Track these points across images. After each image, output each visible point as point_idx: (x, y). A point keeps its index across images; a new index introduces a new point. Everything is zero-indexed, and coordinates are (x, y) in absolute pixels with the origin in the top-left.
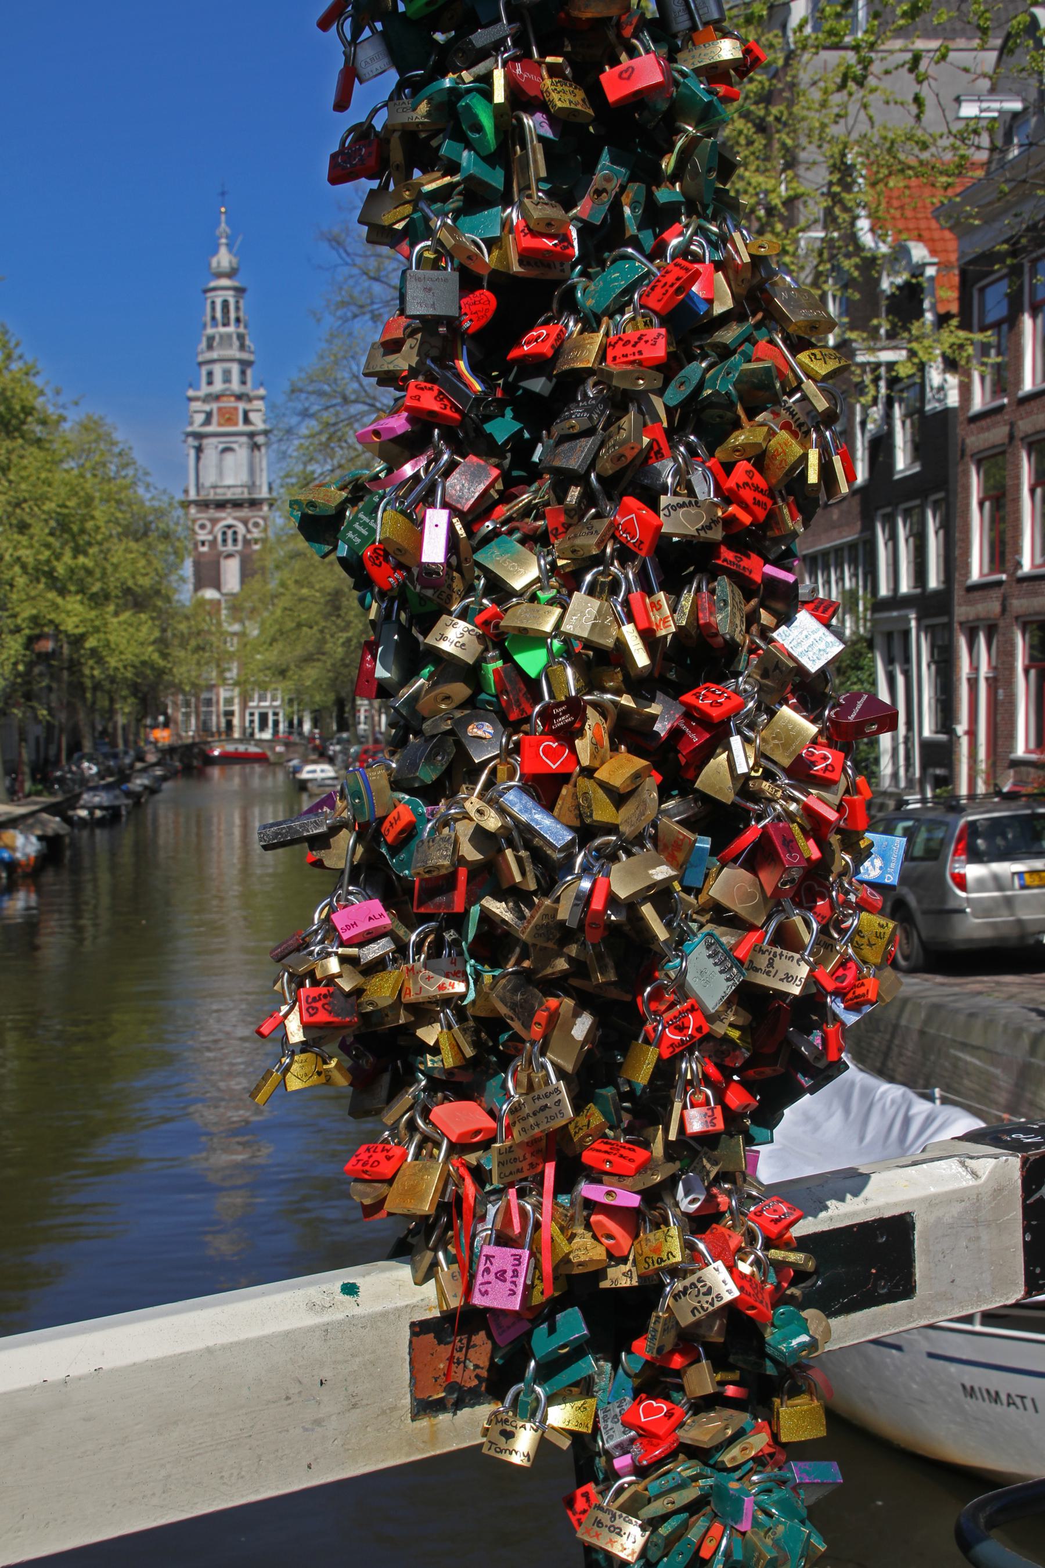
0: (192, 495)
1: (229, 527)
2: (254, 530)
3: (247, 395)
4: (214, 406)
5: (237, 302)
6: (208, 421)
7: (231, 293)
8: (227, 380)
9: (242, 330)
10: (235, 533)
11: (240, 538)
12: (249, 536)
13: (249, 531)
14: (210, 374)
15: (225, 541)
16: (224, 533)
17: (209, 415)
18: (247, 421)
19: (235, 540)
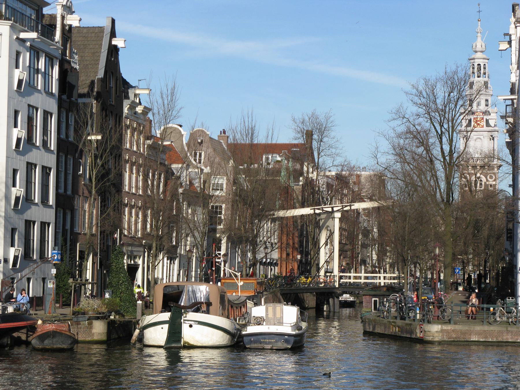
2: (490, 180)
3: (489, 112)
4: (472, 117)
7: (482, 60)
10: (481, 180)
11: (483, 183)
12: (487, 183)
13: (487, 180)
18: (488, 125)
19: (481, 184)
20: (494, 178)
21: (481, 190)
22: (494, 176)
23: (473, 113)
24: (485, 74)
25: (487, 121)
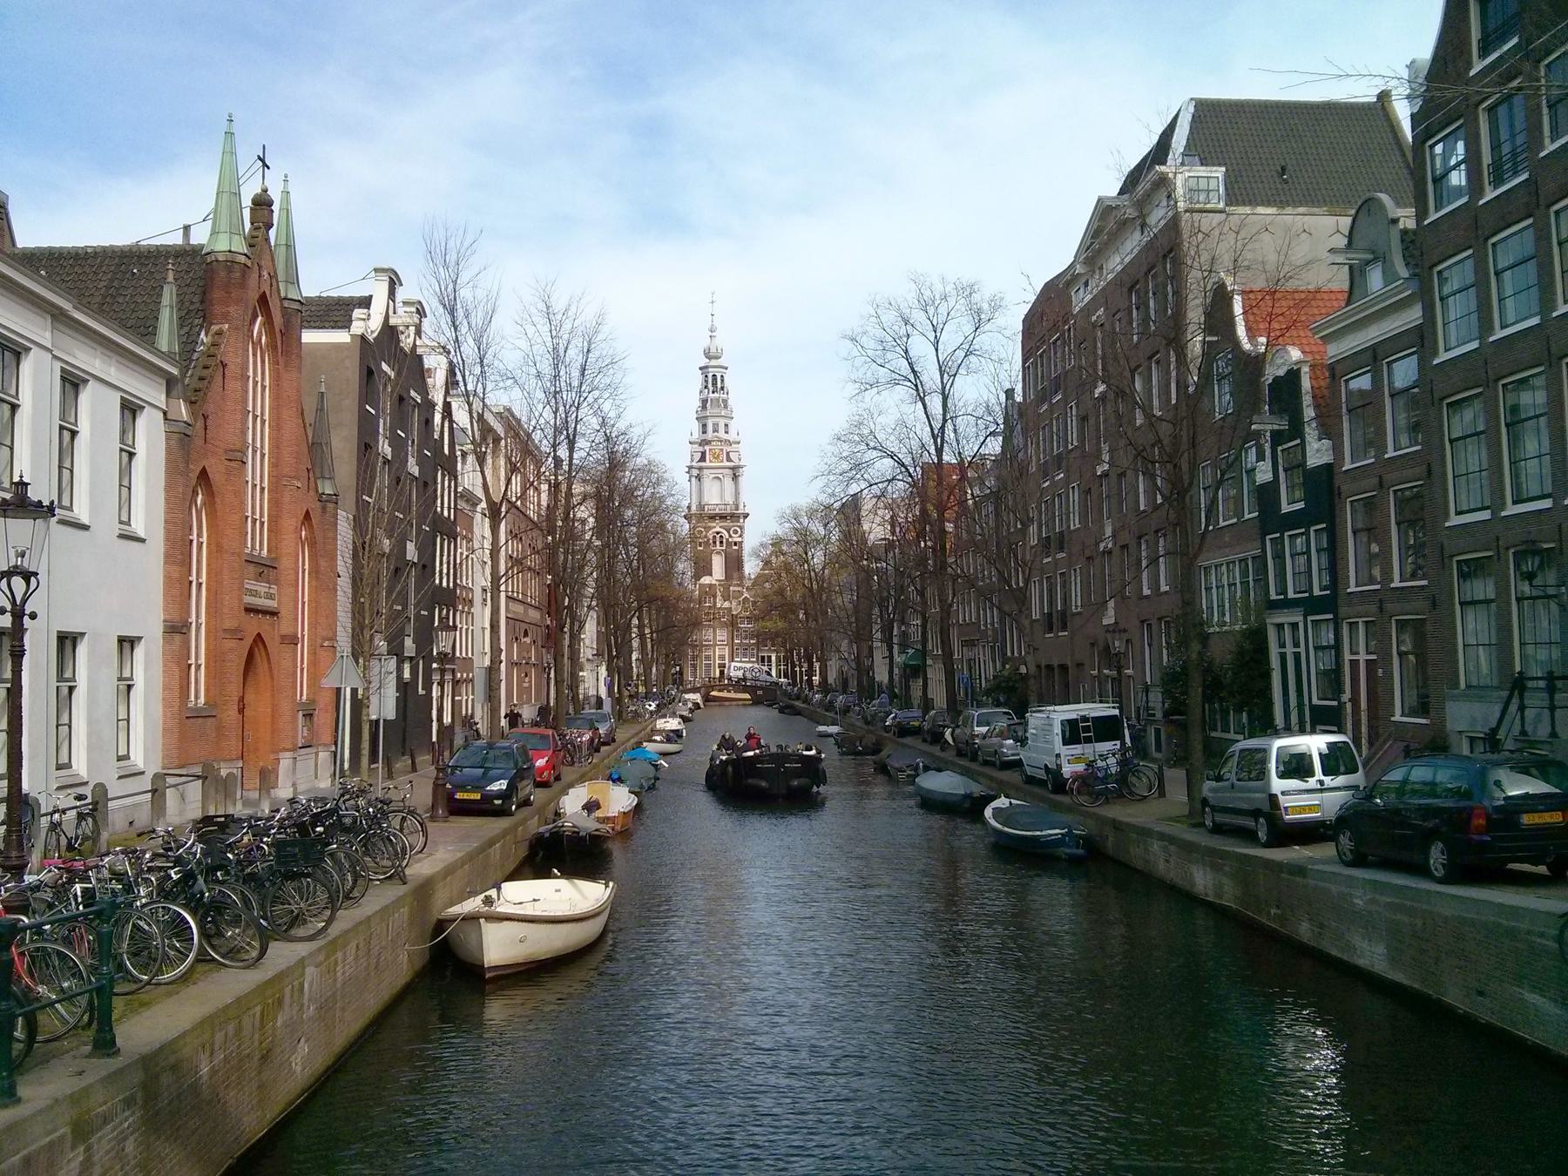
1: (718, 533)
4: (707, 448)
6: (703, 459)
8: (715, 431)
9: (725, 396)
10: (721, 537)
14: (704, 426)
15: (715, 542)
17: (703, 454)
18: (729, 459)
19: (721, 542)
23: (707, 442)
24: (722, 388)
25: (728, 453)
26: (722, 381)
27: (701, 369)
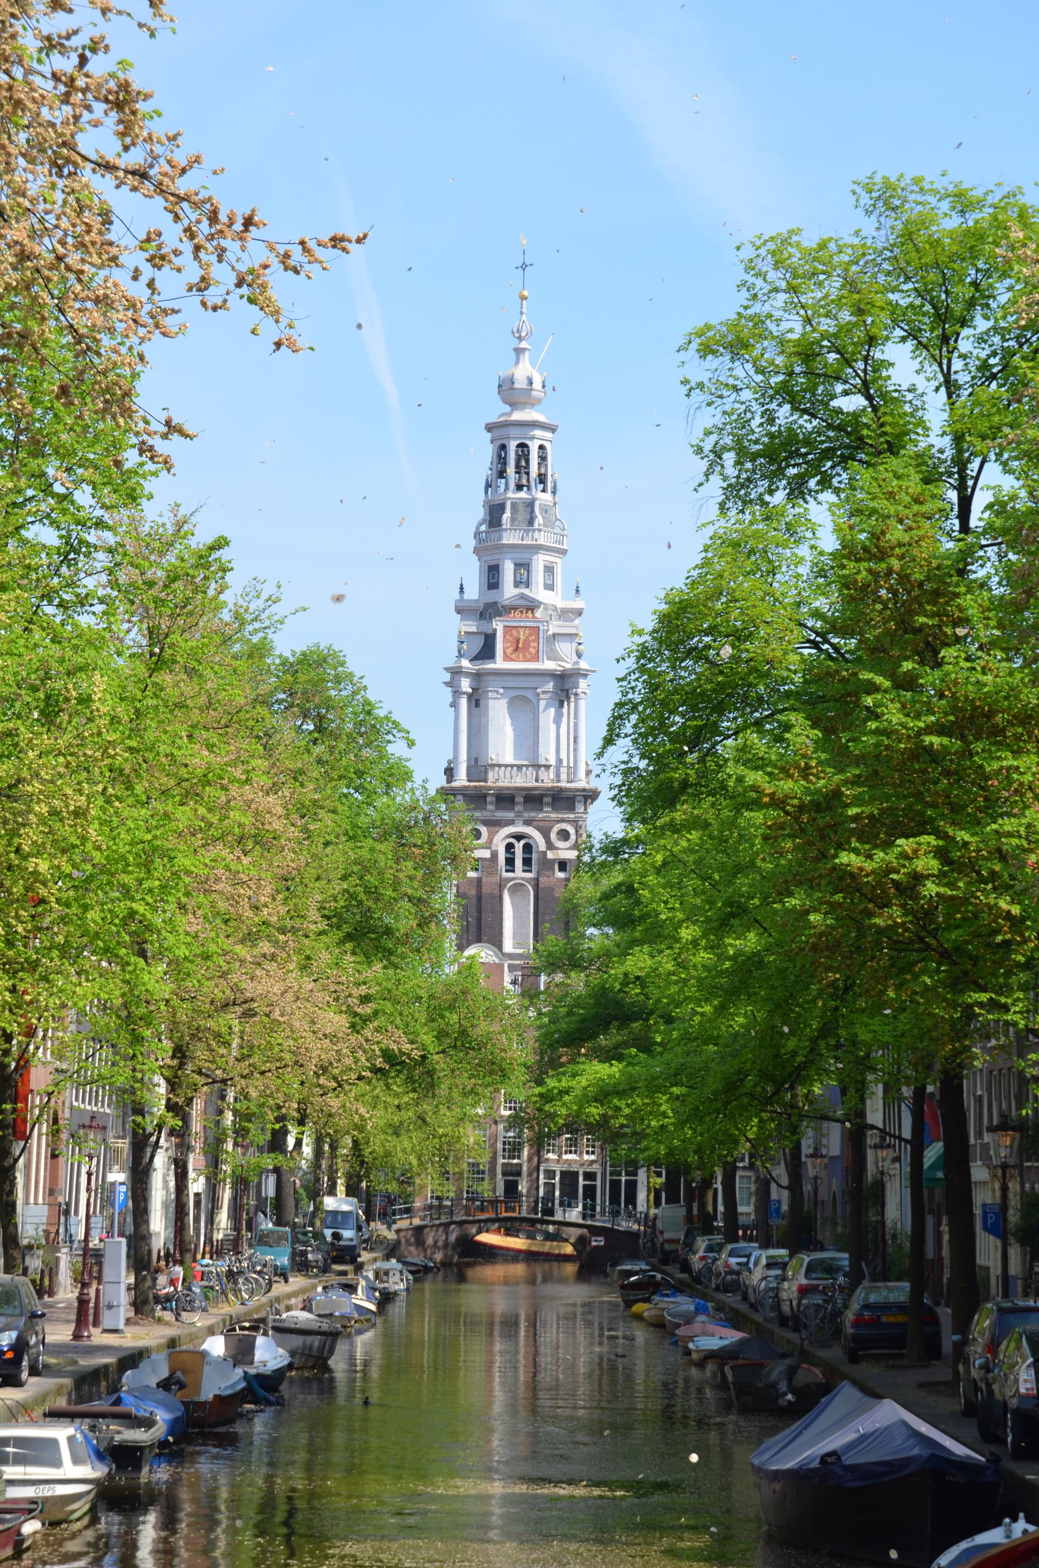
0: (461, 779)
1: (519, 837)
2: (559, 844)
5: (541, 447)
10: (528, 848)
12: (550, 855)
15: (510, 862)
16: (510, 847)
19: (527, 862)
20: (573, 837)
21: (528, 880)
22: (572, 830)
24: (542, 479)
26: (543, 458)
27: (489, 428)
